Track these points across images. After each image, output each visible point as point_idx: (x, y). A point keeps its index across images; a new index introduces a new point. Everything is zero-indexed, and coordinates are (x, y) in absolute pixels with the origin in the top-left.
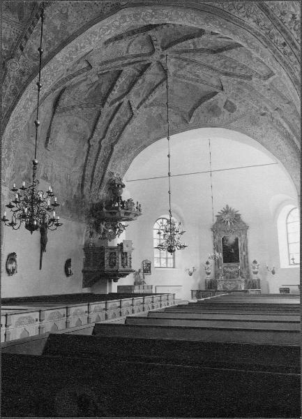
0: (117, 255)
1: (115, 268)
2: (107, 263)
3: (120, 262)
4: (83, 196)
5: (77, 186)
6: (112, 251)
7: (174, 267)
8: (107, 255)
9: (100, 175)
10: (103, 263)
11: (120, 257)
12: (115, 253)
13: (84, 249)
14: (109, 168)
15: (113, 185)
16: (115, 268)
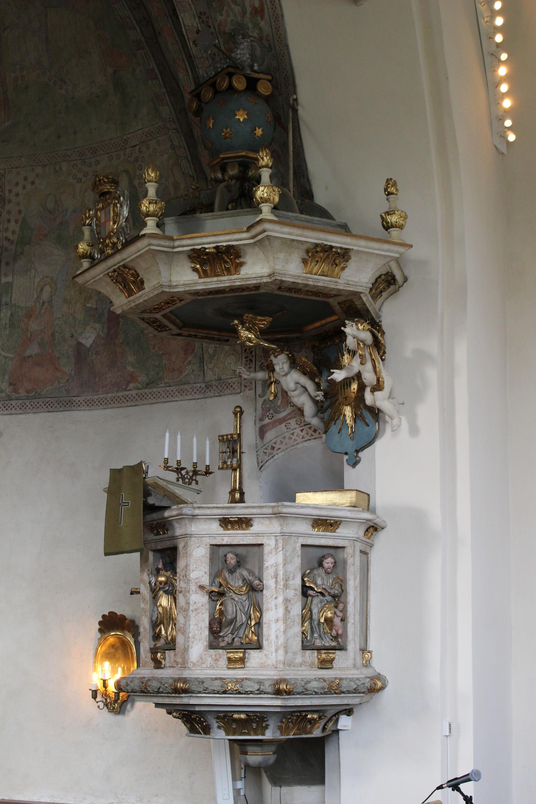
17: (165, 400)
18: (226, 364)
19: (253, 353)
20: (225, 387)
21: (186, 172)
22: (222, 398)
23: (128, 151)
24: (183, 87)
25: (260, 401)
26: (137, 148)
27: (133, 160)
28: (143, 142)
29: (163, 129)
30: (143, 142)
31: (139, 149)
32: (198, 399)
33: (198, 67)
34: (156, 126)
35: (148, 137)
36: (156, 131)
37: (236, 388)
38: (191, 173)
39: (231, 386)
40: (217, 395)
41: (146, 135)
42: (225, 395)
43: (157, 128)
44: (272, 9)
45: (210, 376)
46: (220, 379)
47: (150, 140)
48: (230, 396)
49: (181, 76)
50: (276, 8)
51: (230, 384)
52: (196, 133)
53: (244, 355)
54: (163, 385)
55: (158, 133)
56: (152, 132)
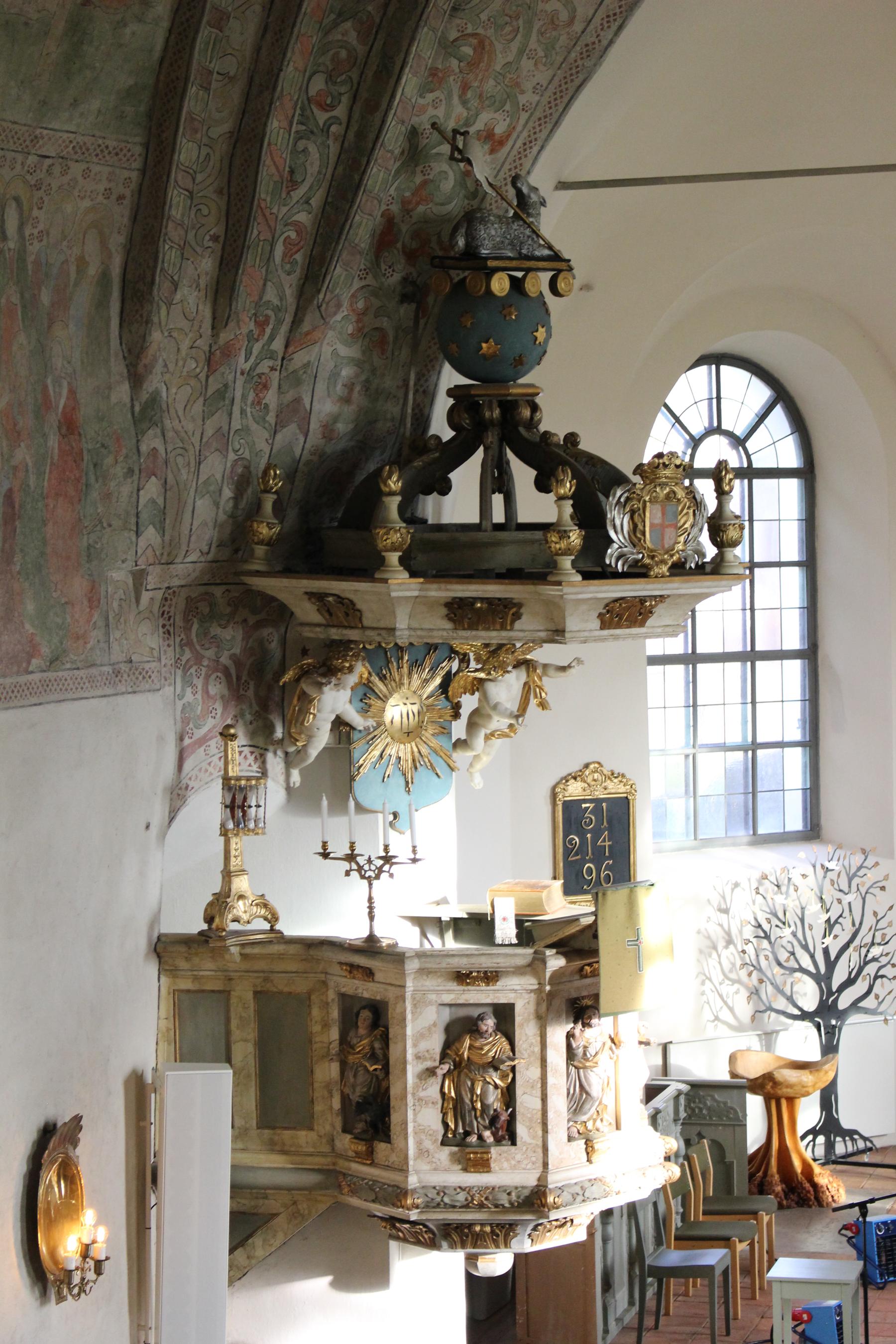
0: (526, 1031)
1: (509, 1171)
2: (420, 1115)
3: (558, 1104)
4: (148, 414)
5: (83, 299)
6: (482, 995)
7: (813, 831)
8: (419, 1034)
9: (316, 160)
10: (373, 1116)
11: (557, 1056)
12: (504, 1015)
13: (166, 949)
14: (409, 83)
15: (442, 263)
16: (509, 1171)
17: (75, 696)
18: (140, 635)
19: (172, 621)
20: (141, 677)
21: (170, 272)
22: (138, 698)
23: (32, 160)
24: (269, 144)
25: (180, 704)
26: (48, 162)
27: (33, 182)
28: (62, 158)
29: (110, 153)
30: (62, 158)
31: (50, 166)
32: (109, 696)
33: (376, 160)
34: (100, 141)
35: (76, 153)
36: (95, 150)
37: (156, 681)
38: (176, 278)
39: (150, 677)
40: (130, 690)
41: (74, 147)
42: (140, 692)
43: (99, 146)
44: (519, 153)
45: (117, 655)
46: (131, 662)
47: (77, 161)
48: (148, 694)
49: (276, 124)
50: (526, 156)
51: (147, 672)
52: (255, 232)
53: (161, 622)
54: (68, 666)
55: (97, 155)
56: (88, 150)
